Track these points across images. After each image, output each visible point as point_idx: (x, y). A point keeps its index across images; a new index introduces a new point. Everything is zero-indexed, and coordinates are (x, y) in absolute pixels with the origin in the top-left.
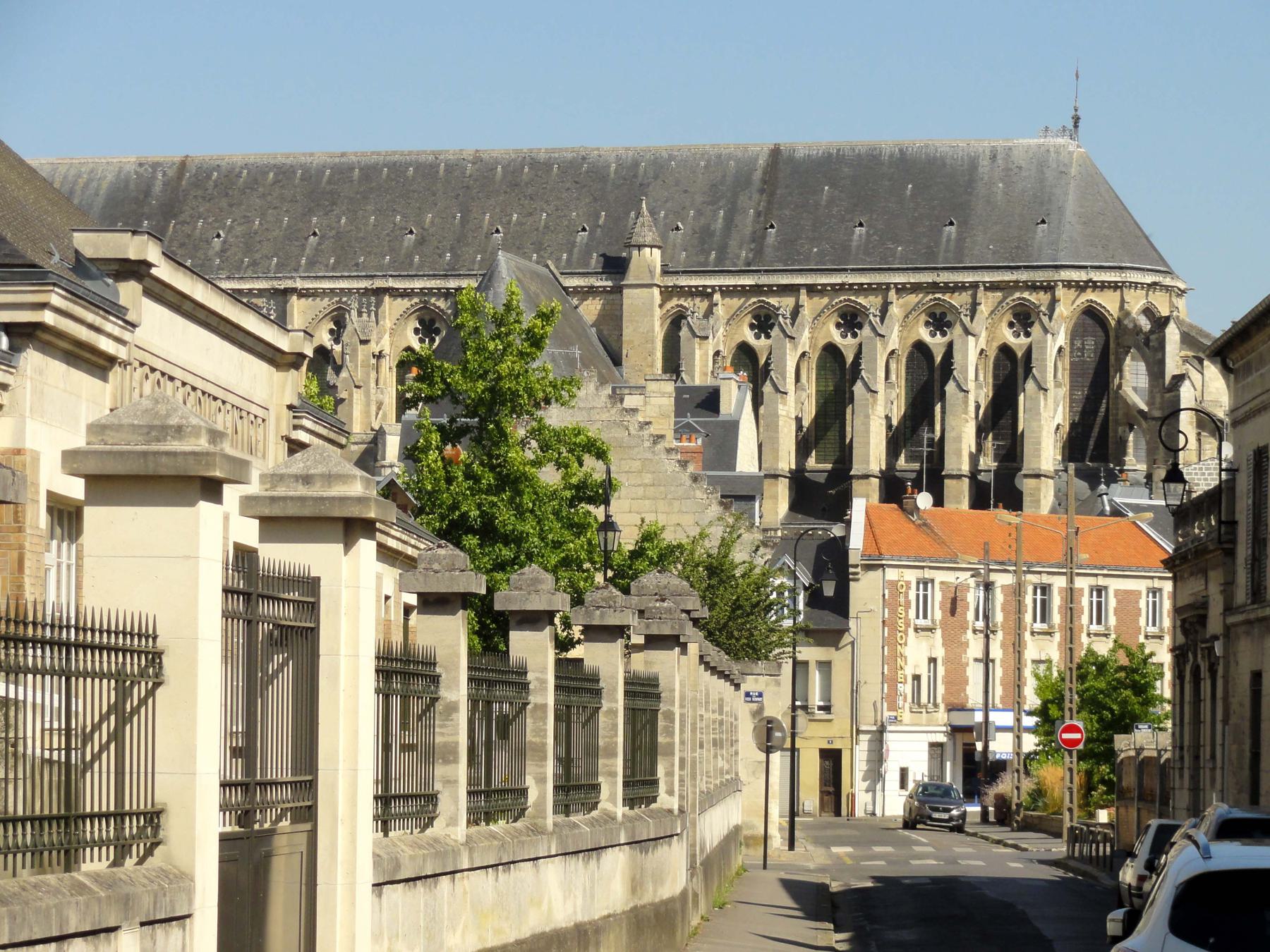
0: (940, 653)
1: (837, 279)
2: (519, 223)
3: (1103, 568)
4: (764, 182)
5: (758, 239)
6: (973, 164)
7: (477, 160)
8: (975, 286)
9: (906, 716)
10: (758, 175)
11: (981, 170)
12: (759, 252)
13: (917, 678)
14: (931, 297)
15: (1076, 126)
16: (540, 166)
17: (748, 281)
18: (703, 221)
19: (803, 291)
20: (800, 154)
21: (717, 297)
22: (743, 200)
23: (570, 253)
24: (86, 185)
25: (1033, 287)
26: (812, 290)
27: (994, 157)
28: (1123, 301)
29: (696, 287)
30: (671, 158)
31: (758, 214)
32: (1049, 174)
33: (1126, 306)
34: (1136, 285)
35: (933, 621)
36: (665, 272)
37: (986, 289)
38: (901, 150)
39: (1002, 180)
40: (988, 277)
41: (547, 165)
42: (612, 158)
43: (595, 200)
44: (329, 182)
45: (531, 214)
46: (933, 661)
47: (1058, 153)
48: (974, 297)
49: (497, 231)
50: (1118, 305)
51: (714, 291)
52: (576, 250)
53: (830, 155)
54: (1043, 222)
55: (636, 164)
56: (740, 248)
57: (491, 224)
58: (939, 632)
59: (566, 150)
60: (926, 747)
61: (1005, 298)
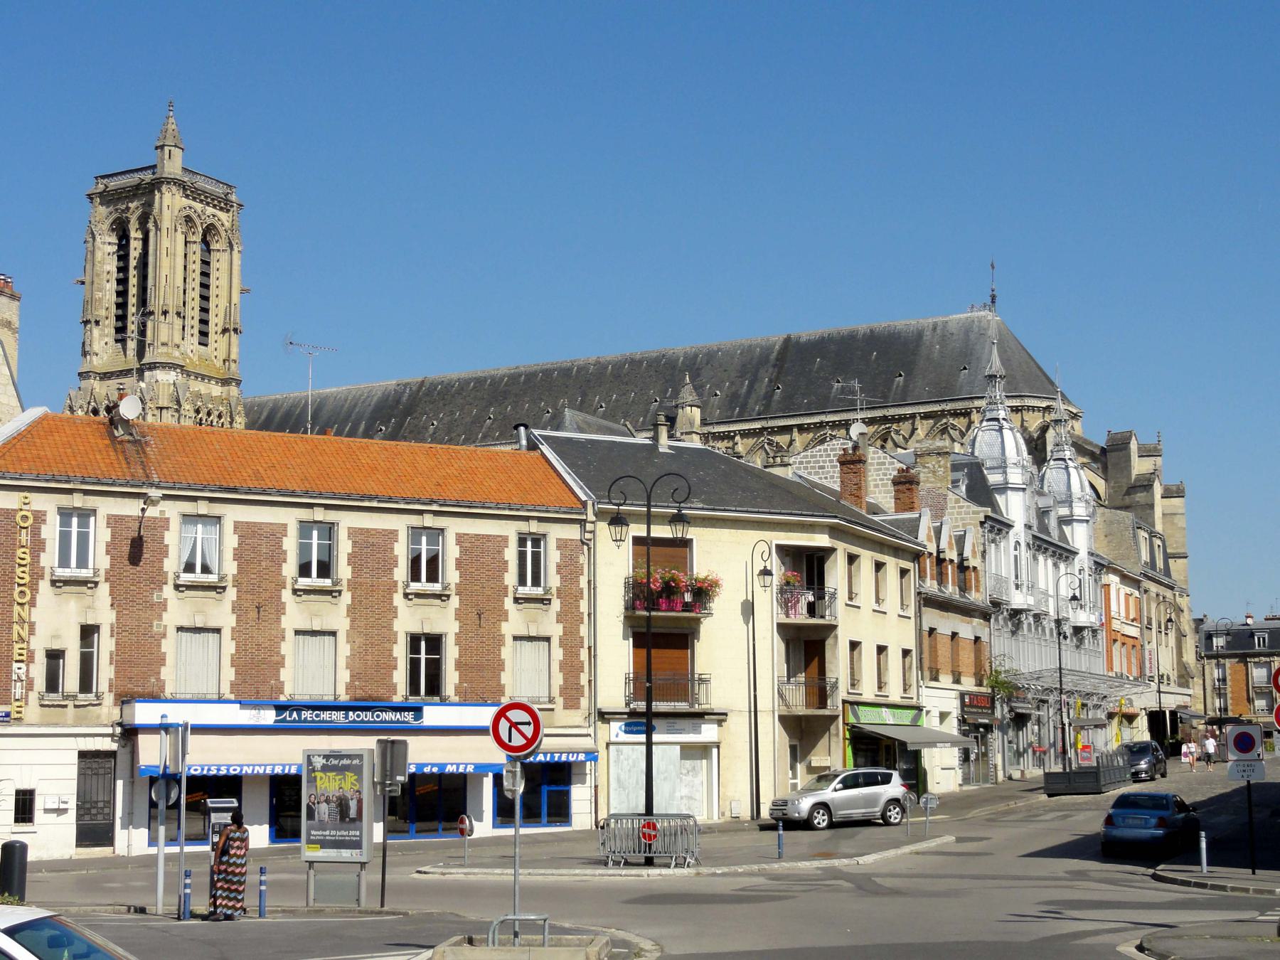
0: (105, 616)
1: (816, 419)
2: (617, 400)
3: (432, 502)
4: (777, 359)
5: (769, 396)
6: (919, 335)
7: (597, 363)
8: (913, 416)
9: (32, 711)
10: (775, 354)
11: (925, 338)
12: (767, 408)
13: (55, 656)
14: (883, 427)
15: (993, 302)
16: (634, 363)
17: (757, 425)
18: (734, 389)
19: (795, 430)
20: (803, 339)
21: (738, 438)
22: (762, 372)
23: (645, 417)
24: (365, 400)
25: (955, 414)
26: (801, 428)
27: (935, 329)
28: (1023, 420)
29: (724, 432)
30: (719, 350)
31: (770, 381)
32: (972, 336)
33: (1025, 424)
34: (1033, 408)
35: (96, 571)
36: (704, 422)
37: (922, 418)
38: (871, 330)
39: (939, 343)
40: (922, 409)
41: (640, 362)
42: (682, 354)
43: (667, 381)
44: (506, 385)
45: (624, 394)
46: (88, 632)
47: (980, 321)
48: (913, 424)
49: (601, 407)
50: (1020, 423)
51: (735, 435)
52: (649, 415)
53: (823, 338)
54: (965, 368)
55: (696, 356)
56: (756, 404)
57: (598, 402)
58: (104, 588)
59: (653, 352)
60: (74, 758)
61: (935, 424)
